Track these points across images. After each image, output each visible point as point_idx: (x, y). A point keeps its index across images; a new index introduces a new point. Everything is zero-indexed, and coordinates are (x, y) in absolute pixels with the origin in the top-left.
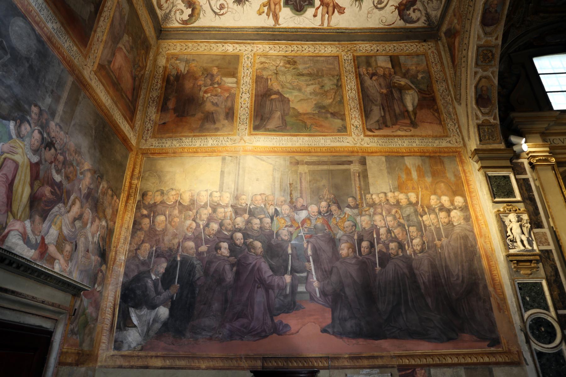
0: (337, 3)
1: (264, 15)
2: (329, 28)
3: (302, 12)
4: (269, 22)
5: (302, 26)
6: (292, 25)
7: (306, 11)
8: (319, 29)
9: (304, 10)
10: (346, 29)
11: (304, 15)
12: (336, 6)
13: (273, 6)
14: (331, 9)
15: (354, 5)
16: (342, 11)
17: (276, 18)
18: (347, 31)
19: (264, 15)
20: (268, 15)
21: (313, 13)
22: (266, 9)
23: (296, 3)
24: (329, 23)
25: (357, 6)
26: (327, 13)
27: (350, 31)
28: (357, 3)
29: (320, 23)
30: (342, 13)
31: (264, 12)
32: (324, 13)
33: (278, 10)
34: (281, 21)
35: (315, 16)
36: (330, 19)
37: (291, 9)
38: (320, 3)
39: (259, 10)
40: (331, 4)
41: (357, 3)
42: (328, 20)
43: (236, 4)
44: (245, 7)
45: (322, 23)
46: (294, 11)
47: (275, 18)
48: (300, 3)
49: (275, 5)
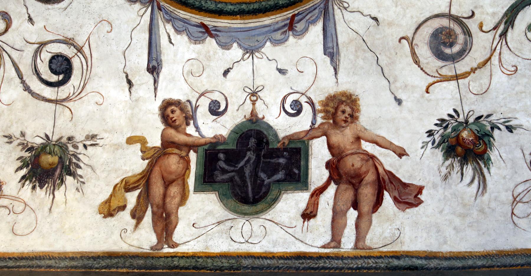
0: (390, 174)
1: (125, 216)
2: (362, 253)
3: (260, 206)
4: (143, 238)
5: (256, 249)
6: (219, 245)
7: (275, 200)
8: (320, 257)
9: (269, 197)
10: (430, 256)
11: (270, 214)
12: (386, 182)
13: (157, 189)
14: (367, 193)
15: (455, 175)
16: (409, 196)
17: (165, 225)
18: (433, 264)
19: (125, 216)
20: (137, 215)
21: (303, 205)
22: (132, 198)
23: (244, 181)
24: (360, 236)
25: (468, 178)
26: (355, 205)
27: (445, 264)
28: (469, 170)
29: (327, 238)
30: (411, 205)
31: (123, 208)
32: (341, 206)
33: (177, 200)
34: (180, 233)
35: (308, 215)
36: (363, 225)
37: (222, 198)
38: (326, 174)
39: (108, 202)
40: (370, 177)
41: (469, 170)
42: (357, 226)
43: (28, 186)
44: (59, 194)
45: (336, 239)
46: (232, 202)
47: (160, 225)
48: (255, 175)
49: (167, 184)
